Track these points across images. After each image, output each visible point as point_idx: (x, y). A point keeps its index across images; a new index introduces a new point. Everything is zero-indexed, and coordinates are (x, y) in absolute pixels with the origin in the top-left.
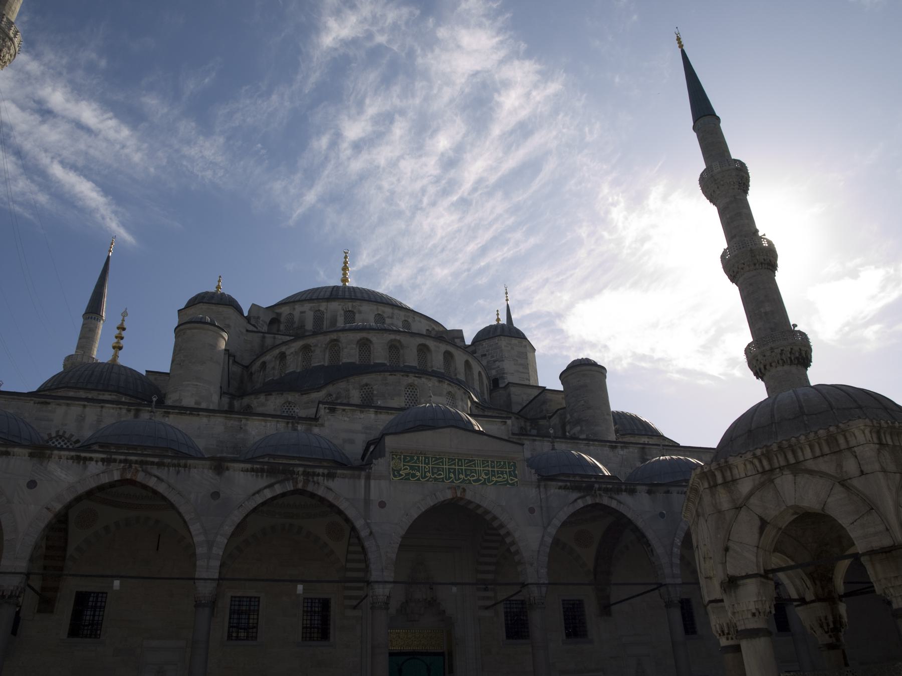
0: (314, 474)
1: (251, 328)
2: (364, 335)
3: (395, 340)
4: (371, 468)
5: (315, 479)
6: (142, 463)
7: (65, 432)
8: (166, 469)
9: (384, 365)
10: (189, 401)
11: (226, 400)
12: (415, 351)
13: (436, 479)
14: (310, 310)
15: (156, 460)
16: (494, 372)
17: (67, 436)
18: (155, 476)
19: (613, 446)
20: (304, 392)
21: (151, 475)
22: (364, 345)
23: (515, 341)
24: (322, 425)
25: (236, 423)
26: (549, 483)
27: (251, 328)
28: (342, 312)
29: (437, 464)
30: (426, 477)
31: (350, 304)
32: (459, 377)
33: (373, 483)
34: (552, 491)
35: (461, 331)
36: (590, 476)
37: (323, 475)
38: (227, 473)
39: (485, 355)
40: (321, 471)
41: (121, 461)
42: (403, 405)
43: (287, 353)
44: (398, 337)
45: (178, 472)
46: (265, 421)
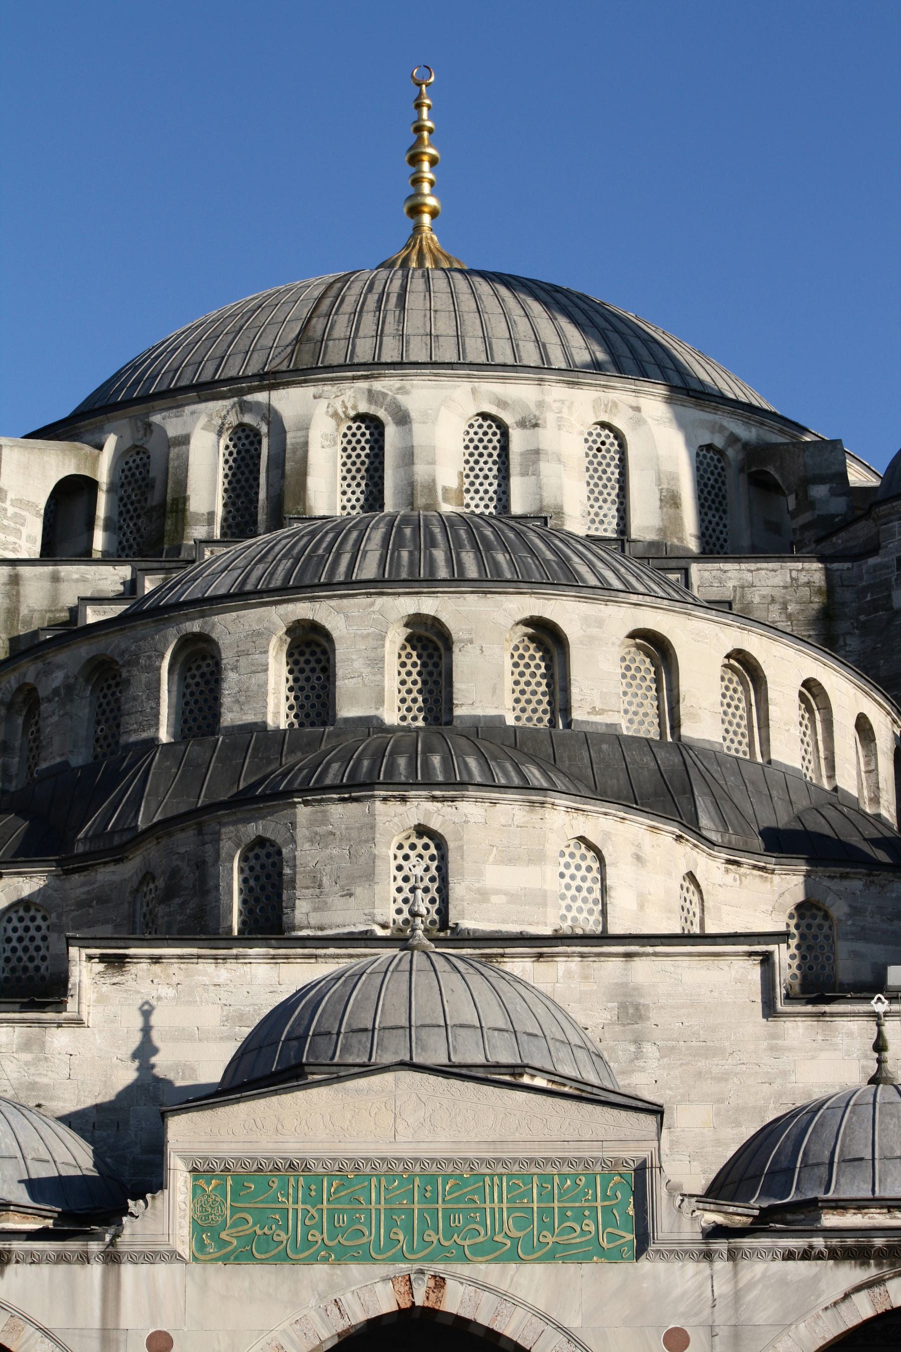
9: (371, 725)
24: (78, 1022)
26: (746, 1242)
43: (42, 693)
44: (428, 605)
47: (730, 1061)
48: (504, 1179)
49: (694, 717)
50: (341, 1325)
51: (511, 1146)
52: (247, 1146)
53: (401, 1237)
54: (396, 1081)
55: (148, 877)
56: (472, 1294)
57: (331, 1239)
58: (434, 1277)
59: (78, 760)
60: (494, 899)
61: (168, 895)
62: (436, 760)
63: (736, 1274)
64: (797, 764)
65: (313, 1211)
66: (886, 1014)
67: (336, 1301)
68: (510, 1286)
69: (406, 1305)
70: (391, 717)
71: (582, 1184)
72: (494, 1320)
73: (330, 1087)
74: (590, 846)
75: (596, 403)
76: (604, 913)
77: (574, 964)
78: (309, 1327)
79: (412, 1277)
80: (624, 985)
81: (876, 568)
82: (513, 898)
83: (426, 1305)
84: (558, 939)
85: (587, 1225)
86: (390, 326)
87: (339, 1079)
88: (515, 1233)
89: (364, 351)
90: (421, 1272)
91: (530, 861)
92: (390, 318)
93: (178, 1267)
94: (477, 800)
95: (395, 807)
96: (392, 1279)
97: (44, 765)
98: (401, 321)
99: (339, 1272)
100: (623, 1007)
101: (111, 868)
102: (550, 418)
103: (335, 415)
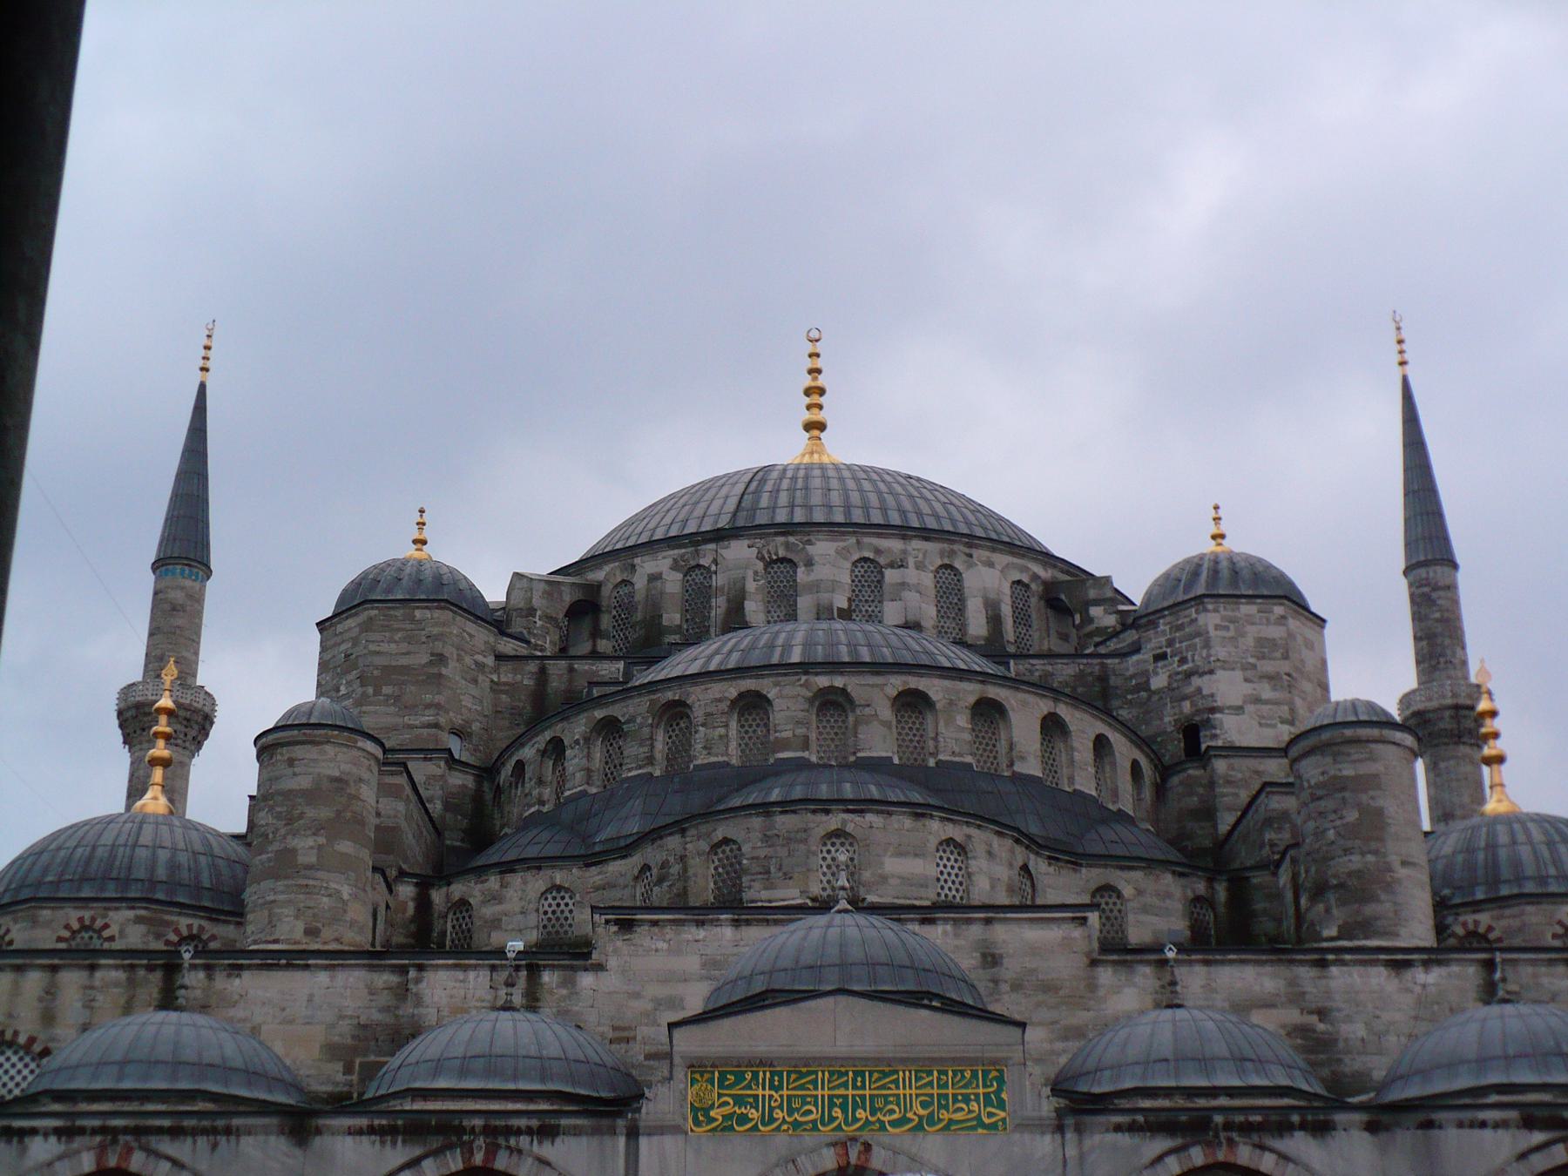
0: (510, 1131)
1: (508, 646)
2: (749, 684)
3: (831, 689)
4: (639, 1110)
5: (512, 1142)
6: (138, 1132)
7: (16, 1033)
8: (189, 1140)
9: (802, 765)
10: (290, 932)
11: (406, 891)
12: (887, 713)
13: (796, 1125)
14: (675, 566)
15: (166, 1123)
16: (1187, 706)
17: (22, 1039)
18: (169, 1158)
19: (1399, 962)
20: (591, 860)
21: (159, 1155)
22: (753, 705)
23: (1247, 609)
25: (394, 979)
26: (1088, 1119)
27: (508, 646)
28: (760, 566)
29: (802, 1087)
30: (772, 1120)
31: (781, 539)
32: (1019, 768)
33: (643, 1142)
34: (1097, 1138)
35: (1108, 580)
36: (1213, 1092)
37: (530, 1131)
38: (317, 1141)
39: (1163, 657)
40: (522, 1122)
41: (94, 1131)
42: (815, 890)
44: (839, 682)
45: (215, 1146)
46: (465, 968)
49: (1022, 758)
53: (839, 1114)
55: (646, 868)
59: (594, 790)
60: (891, 881)
61: (660, 881)
62: (848, 785)
63: (1080, 1142)
64: (1094, 793)
66: (1176, 961)
69: (843, 1163)
70: (814, 759)
74: (957, 845)
75: (942, 554)
76: (967, 891)
77: (949, 928)
80: (985, 940)
81: (1138, 662)
82: (906, 880)
84: (936, 907)
86: (798, 501)
87: (795, 1001)
88: (922, 1112)
89: (781, 517)
90: (854, 1139)
91: (916, 855)
92: (798, 493)
93: (680, 1138)
94: (879, 812)
95: (824, 818)
96: (834, 1144)
97: (567, 793)
98: (806, 497)
100: (984, 955)
101: (619, 862)
102: (911, 561)
103: (762, 559)
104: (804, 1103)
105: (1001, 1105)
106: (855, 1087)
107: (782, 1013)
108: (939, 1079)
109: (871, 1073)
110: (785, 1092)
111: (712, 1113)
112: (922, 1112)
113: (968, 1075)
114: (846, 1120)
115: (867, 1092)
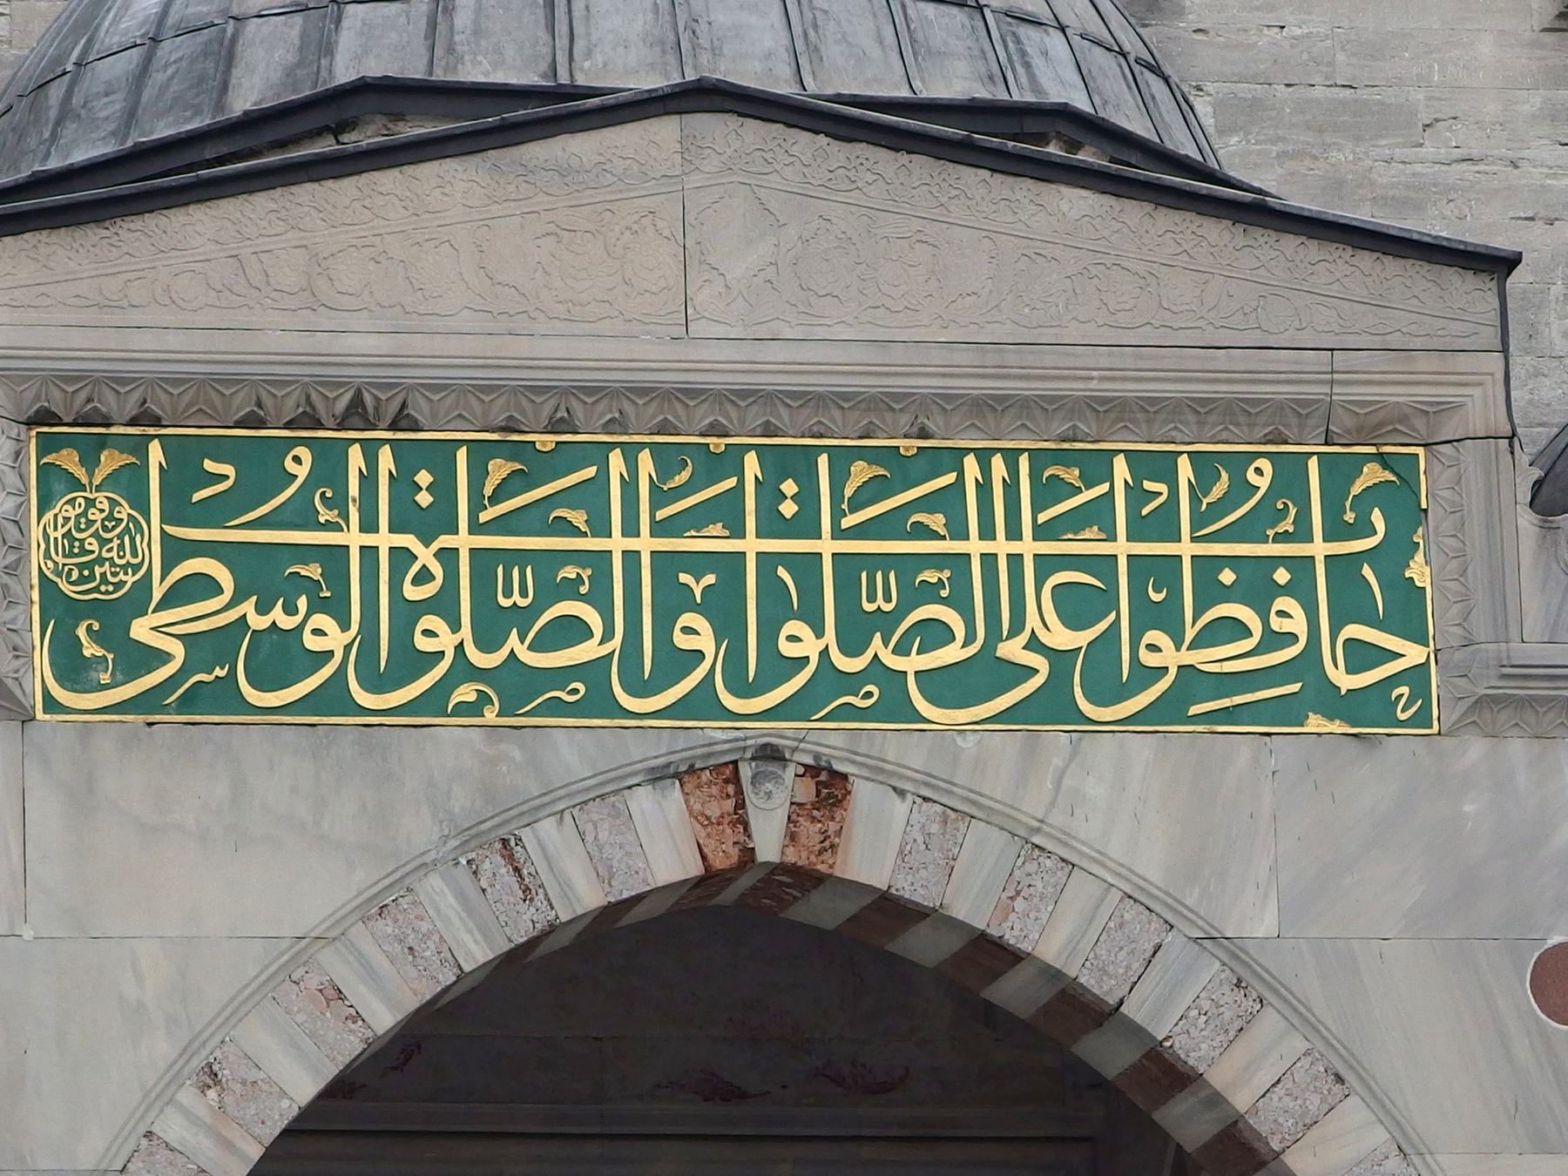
13: (516, 686)
30: (412, 662)
47: (1429, 150)
48: (1024, 462)
50: (523, 925)
51: (1049, 360)
52: (221, 342)
53: (705, 641)
54: (687, 146)
56: (935, 828)
57: (486, 646)
58: (811, 771)
65: (425, 556)
67: (505, 842)
68: (1053, 804)
71: (1263, 483)
72: (1005, 910)
73: (476, 159)
78: (425, 926)
79: (746, 771)
83: (791, 857)
85: (1281, 613)
88: (1061, 637)
90: (770, 754)
99: (517, 754)
104: (552, 591)
105: (1407, 614)
106: (772, 525)
107: (451, 190)
108: (1137, 495)
109: (841, 461)
110: (463, 541)
111: (141, 630)
112: (1061, 637)
113: (1261, 477)
114: (735, 659)
115: (827, 547)
